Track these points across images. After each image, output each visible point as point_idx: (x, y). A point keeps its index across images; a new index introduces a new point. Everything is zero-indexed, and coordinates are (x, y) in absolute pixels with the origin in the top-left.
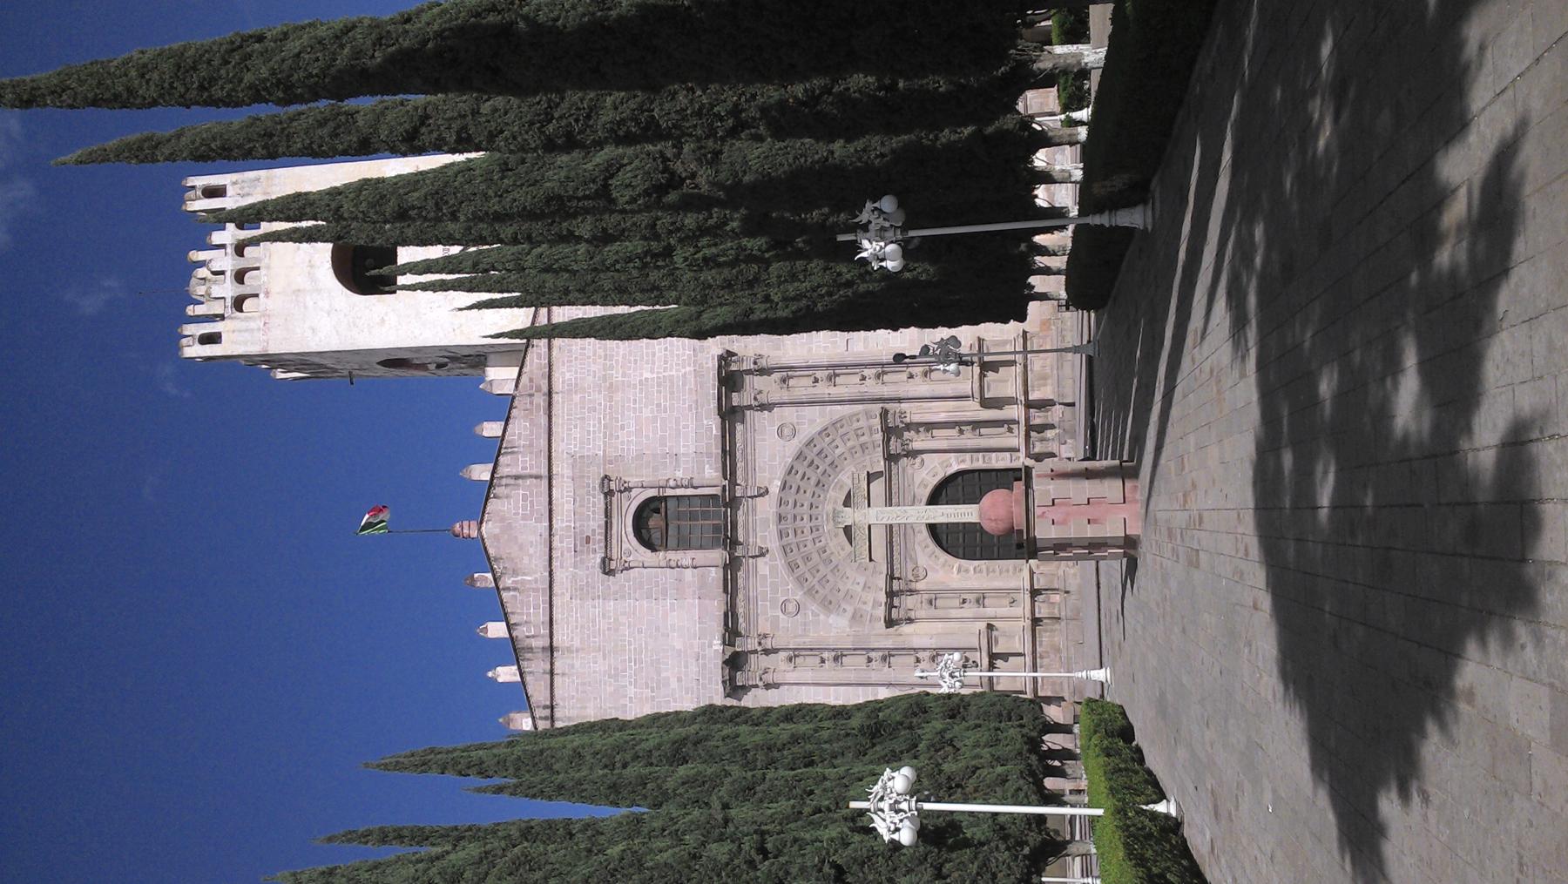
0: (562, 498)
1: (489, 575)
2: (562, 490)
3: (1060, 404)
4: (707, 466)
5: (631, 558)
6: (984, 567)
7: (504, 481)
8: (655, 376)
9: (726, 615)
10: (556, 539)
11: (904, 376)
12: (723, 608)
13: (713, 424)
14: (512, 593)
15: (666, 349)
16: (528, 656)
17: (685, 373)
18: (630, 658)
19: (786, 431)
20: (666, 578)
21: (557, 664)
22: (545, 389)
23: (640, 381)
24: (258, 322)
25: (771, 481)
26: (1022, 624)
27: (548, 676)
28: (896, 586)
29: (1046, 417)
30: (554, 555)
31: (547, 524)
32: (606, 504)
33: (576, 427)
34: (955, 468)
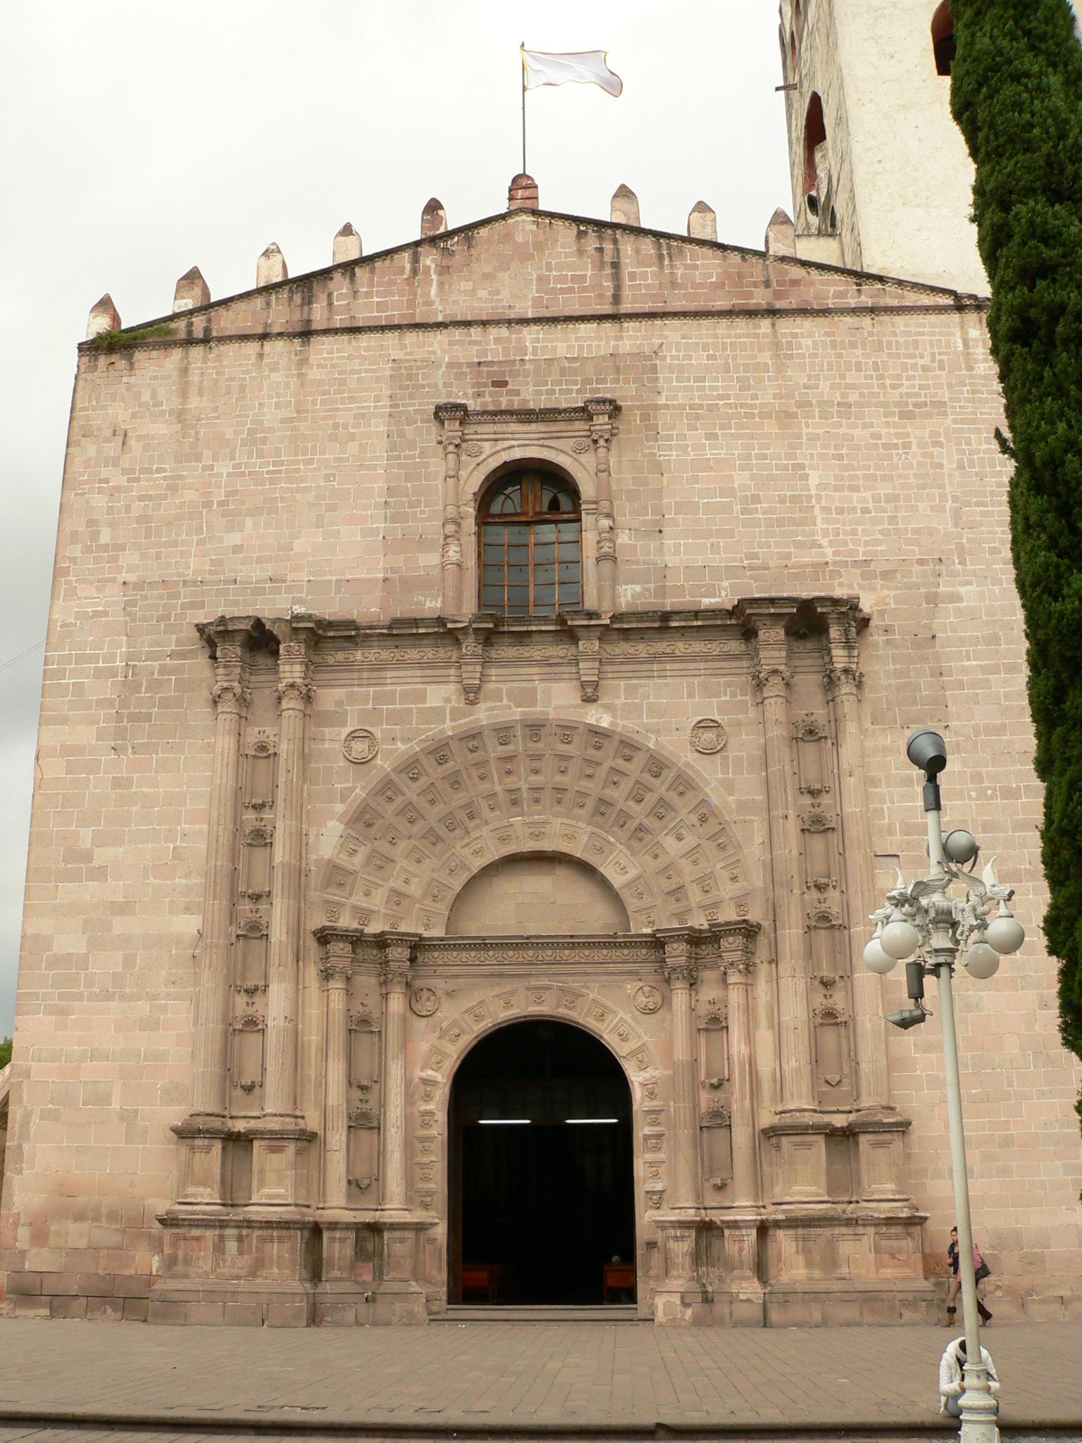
0: (577, 339)
4: (638, 588)
7: (608, 246)
8: (813, 492)
9: (351, 624)
10: (503, 331)
12: (362, 621)
13: (724, 597)
14: (408, 266)
15: (866, 511)
16: (298, 298)
17: (820, 546)
18: (281, 463)
19: (709, 736)
22: (779, 305)
23: (802, 467)
25: (609, 708)
27: (260, 330)
30: (475, 332)
31: (530, 315)
32: (565, 411)
33: (709, 357)
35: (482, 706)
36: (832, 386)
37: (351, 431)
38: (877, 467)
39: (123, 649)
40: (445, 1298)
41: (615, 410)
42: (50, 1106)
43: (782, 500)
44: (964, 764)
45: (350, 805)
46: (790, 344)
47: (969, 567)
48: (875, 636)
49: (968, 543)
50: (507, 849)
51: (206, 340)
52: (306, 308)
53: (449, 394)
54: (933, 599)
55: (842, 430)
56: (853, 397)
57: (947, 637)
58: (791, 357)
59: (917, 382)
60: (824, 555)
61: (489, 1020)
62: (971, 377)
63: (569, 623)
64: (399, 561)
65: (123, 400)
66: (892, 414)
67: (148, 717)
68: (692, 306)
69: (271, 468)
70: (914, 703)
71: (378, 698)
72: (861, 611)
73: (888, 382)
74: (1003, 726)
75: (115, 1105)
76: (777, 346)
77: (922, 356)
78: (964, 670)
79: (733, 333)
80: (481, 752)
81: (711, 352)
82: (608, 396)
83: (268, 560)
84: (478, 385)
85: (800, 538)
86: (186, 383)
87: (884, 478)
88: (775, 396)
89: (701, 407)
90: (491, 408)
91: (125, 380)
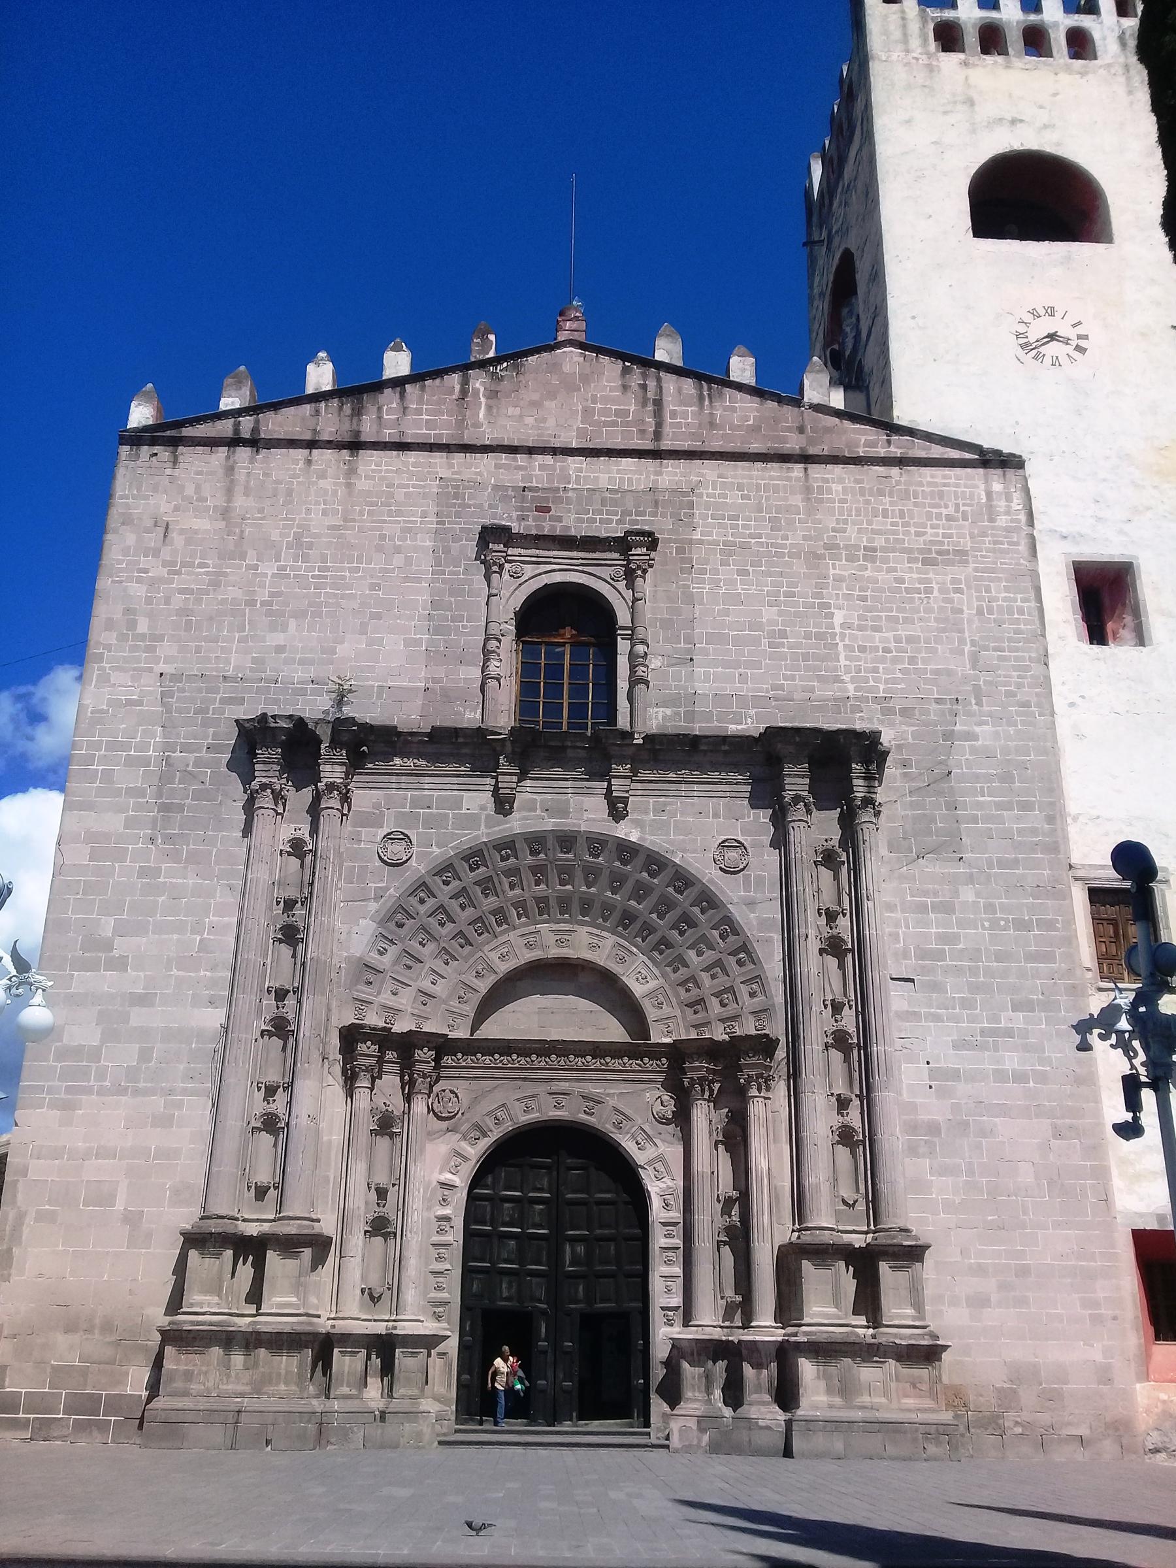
0: (619, 472)
1: (491, 354)
2: (635, 472)
3: (789, 1423)
4: (669, 711)
5: (506, 576)
6: (448, 1238)
7: (652, 384)
8: (838, 630)
10: (549, 459)
11: (840, 1088)
13: (749, 724)
14: (457, 388)
15: (887, 650)
16: (347, 409)
17: (842, 681)
18: (327, 569)
19: (732, 855)
20: (465, 634)
21: (328, 454)
22: (812, 451)
23: (828, 605)
24: (919, 50)
25: (638, 824)
26: (325, 1314)
28: (424, 1054)
29: (758, 1390)
30: (521, 459)
31: (574, 445)
34: (654, 1187)
35: (515, 815)
36: (860, 531)
37: (397, 543)
38: (899, 610)
39: (157, 739)
40: (453, 1418)
41: (652, 541)
42: (47, 1207)
43: (807, 636)
44: (978, 895)
45: (384, 904)
46: (820, 488)
47: (986, 708)
48: (891, 770)
49: (984, 685)
50: (533, 954)
51: (255, 443)
52: (355, 419)
53: (494, 516)
54: (949, 736)
55: (867, 573)
56: (879, 541)
57: (963, 773)
58: (821, 501)
59: (941, 531)
60: (846, 690)
61: (510, 1123)
62: (993, 528)
63: (604, 740)
64: (441, 672)
65: (165, 492)
66: (916, 560)
67: (181, 808)
68: (730, 447)
69: (317, 573)
70: (930, 834)
71: (415, 803)
72: (881, 744)
73: (913, 530)
74: (1016, 861)
75: (119, 1206)
76: (808, 489)
77: (946, 507)
78: (980, 805)
79: (767, 474)
80: (512, 860)
81: (746, 492)
82: (646, 528)
83: (311, 662)
84: (522, 509)
85: (823, 673)
86: (232, 481)
87: (906, 621)
88: (805, 538)
89: (734, 544)
90: (534, 532)
91: (168, 472)
